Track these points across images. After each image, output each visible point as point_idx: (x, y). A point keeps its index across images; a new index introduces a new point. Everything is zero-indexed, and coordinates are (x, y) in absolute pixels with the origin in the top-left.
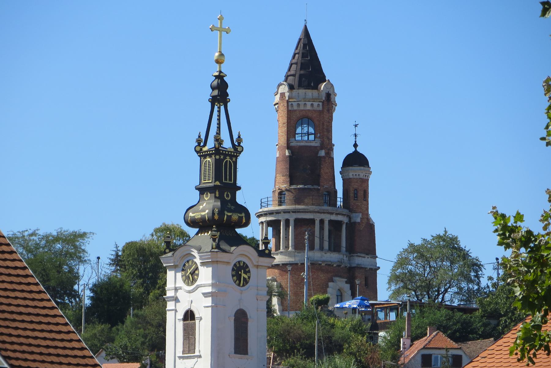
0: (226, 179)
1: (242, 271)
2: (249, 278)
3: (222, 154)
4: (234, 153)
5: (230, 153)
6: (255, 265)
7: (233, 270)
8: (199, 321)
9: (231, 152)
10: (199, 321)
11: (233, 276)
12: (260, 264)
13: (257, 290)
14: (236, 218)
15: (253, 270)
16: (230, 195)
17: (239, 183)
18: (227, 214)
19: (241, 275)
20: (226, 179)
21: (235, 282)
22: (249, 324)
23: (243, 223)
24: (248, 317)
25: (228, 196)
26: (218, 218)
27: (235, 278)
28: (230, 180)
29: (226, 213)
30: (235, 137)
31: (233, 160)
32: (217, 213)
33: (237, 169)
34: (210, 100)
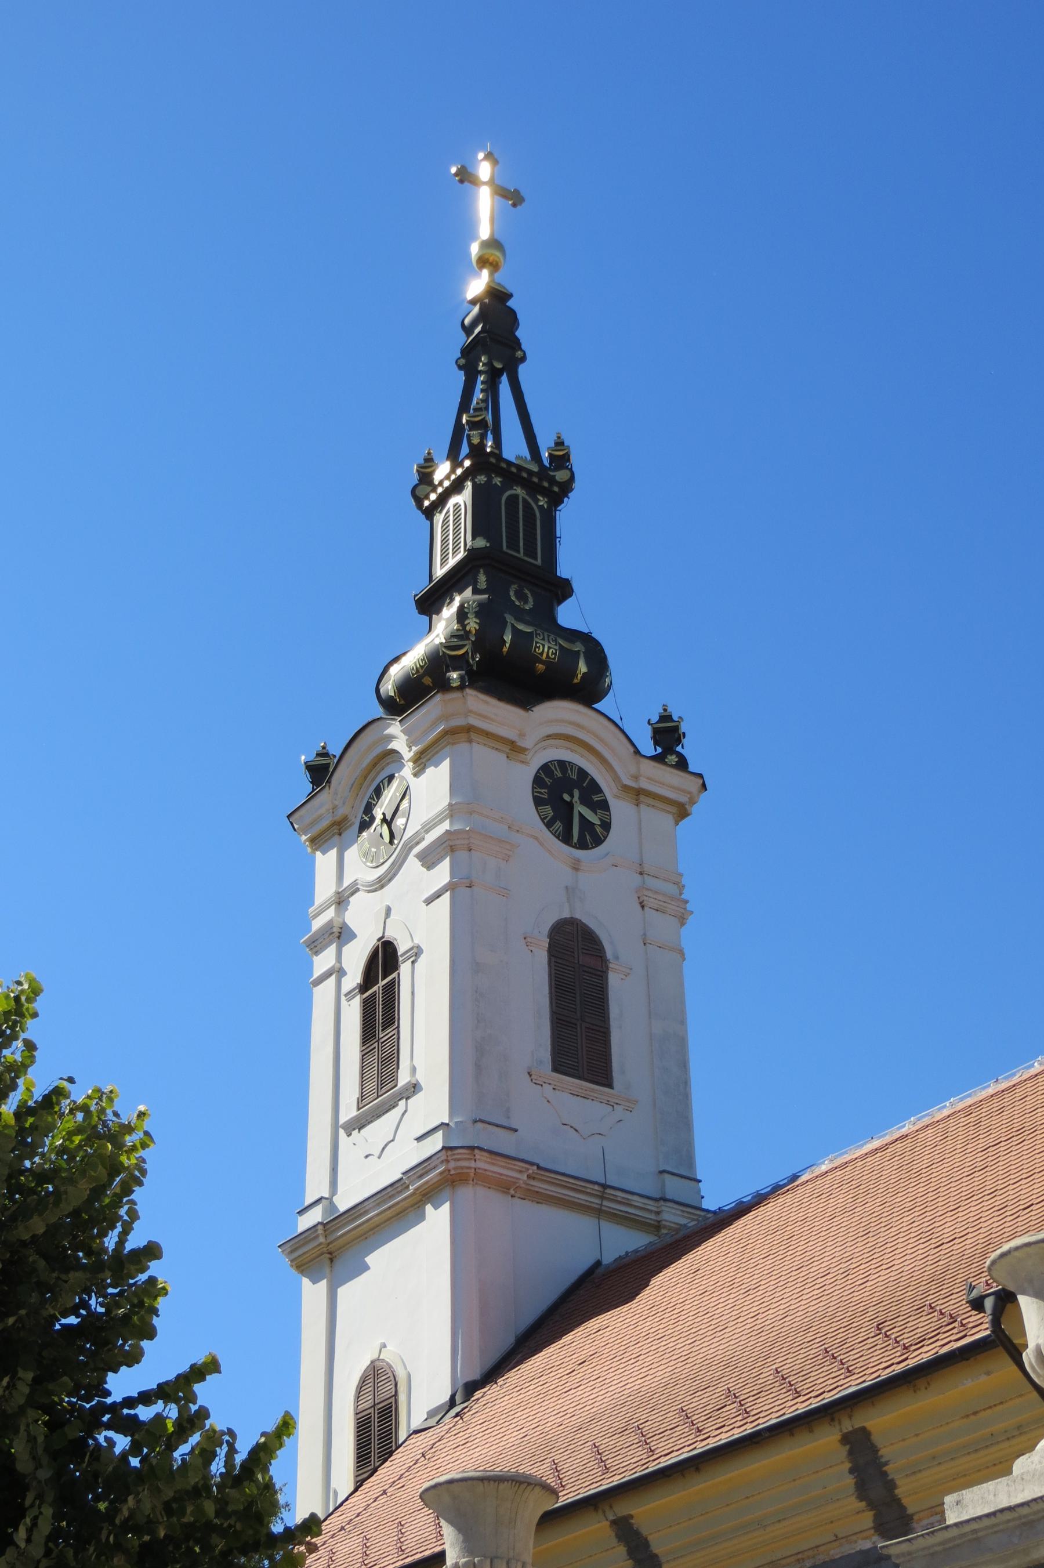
0: (513, 544)
1: (576, 793)
2: (607, 826)
4: (540, 479)
5: (525, 475)
6: (626, 788)
7: (538, 781)
8: (413, 962)
9: (530, 473)
10: (413, 962)
11: (538, 802)
12: (645, 784)
13: (641, 873)
14: (549, 648)
15: (620, 809)
16: (529, 595)
17: (563, 570)
19: (570, 806)
20: (513, 544)
22: (614, 980)
23: (579, 676)
24: (609, 954)
25: (522, 597)
26: (477, 628)
27: (549, 810)
28: (531, 552)
29: (509, 619)
32: (475, 612)
33: (558, 540)
34: (462, 362)
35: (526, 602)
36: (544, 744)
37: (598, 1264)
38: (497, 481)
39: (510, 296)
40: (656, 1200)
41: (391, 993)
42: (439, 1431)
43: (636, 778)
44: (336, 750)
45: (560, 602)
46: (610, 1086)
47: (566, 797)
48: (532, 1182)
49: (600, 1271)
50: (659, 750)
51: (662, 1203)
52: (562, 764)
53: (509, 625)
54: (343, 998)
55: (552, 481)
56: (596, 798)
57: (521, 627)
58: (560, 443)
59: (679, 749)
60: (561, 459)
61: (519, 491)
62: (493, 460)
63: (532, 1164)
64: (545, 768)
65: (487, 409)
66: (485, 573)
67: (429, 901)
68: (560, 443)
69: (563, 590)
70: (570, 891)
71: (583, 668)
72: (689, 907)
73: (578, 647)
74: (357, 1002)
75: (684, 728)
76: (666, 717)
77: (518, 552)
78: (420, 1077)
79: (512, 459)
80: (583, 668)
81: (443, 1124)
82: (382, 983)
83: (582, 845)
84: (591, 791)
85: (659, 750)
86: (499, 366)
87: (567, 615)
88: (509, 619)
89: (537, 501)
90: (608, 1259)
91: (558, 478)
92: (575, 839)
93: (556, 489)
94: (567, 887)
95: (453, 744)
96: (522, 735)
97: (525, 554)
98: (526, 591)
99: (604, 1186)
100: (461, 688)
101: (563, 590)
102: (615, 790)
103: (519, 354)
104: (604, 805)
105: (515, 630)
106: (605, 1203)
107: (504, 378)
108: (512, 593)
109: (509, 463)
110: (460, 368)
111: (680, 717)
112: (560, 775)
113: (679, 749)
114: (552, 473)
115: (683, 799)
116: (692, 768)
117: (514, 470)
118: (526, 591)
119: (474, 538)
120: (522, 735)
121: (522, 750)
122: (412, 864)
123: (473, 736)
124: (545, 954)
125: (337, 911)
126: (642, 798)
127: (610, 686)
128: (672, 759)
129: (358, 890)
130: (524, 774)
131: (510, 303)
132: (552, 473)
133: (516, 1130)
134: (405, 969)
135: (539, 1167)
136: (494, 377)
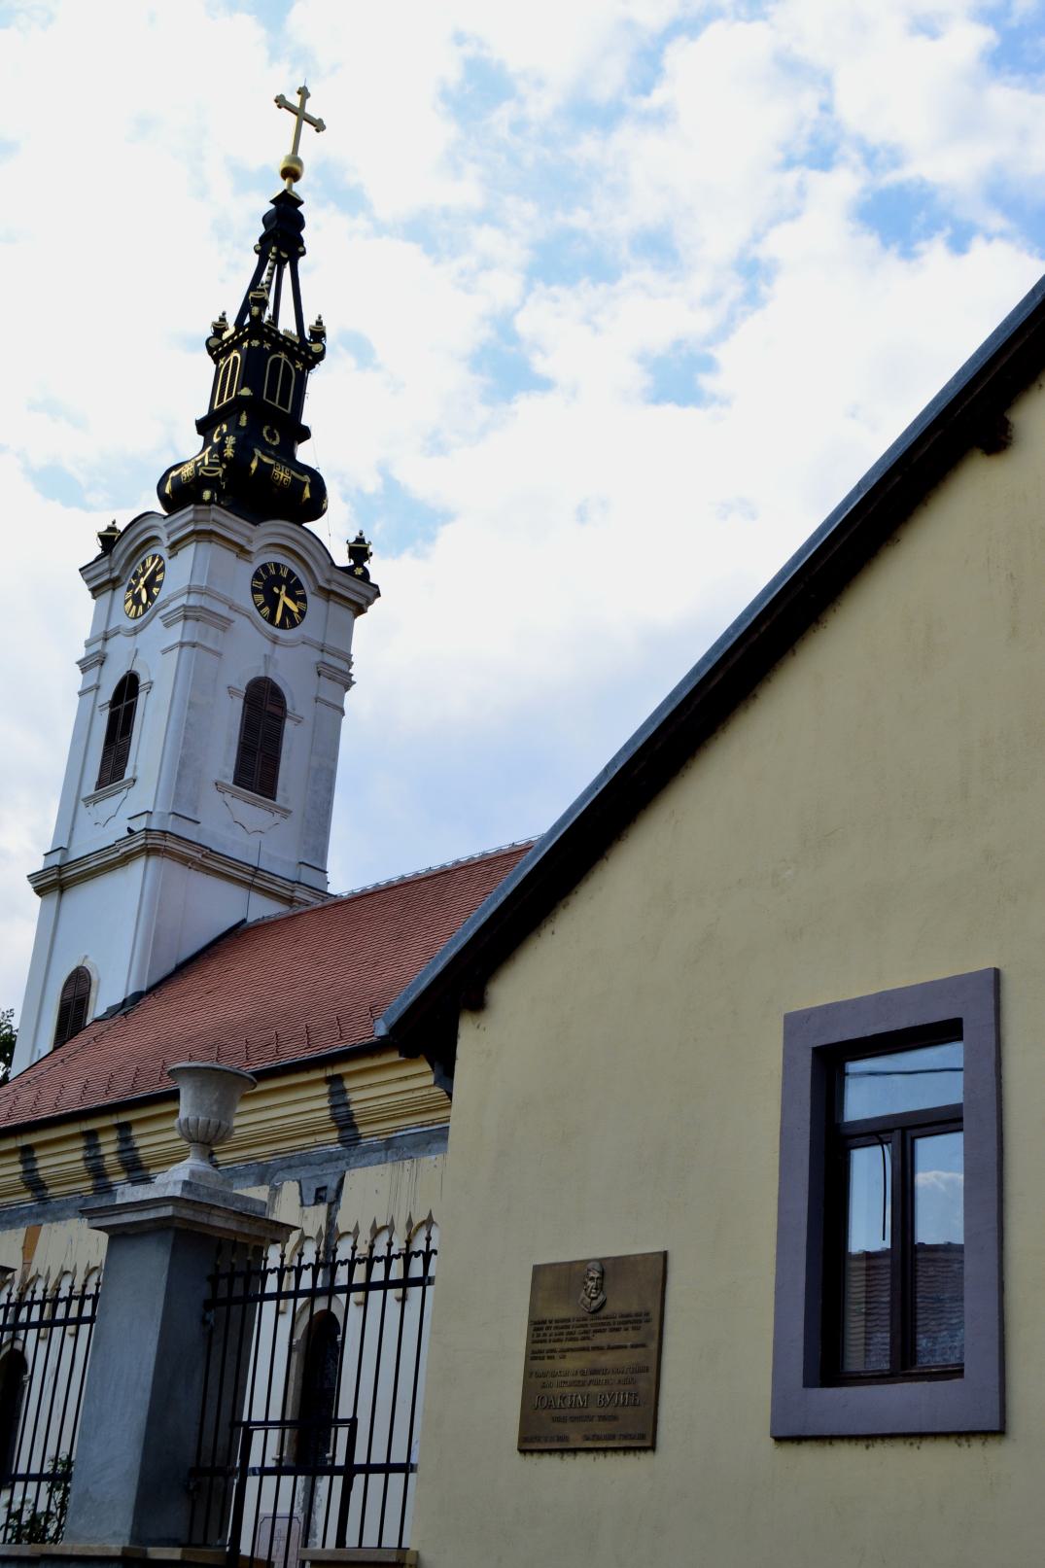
0: (271, 395)
1: (284, 588)
2: (302, 614)
3: (270, 340)
4: (300, 350)
5: (288, 344)
6: (321, 589)
7: (257, 576)
11: (255, 591)
12: (334, 587)
13: (322, 651)
15: (315, 604)
17: (306, 420)
18: (259, 458)
19: (278, 597)
20: (271, 395)
21: (259, 609)
23: (303, 500)
25: (272, 436)
27: (261, 598)
28: (284, 402)
29: (258, 452)
30: (309, 322)
31: (297, 366)
34: (259, 248)
35: (274, 439)
36: (265, 550)
37: (244, 921)
38: (267, 346)
39: (301, 203)
40: (293, 882)
41: (130, 711)
42: (112, 1021)
43: (329, 581)
44: (121, 527)
45: (299, 443)
46: (274, 799)
47: (276, 590)
48: (206, 860)
49: (244, 926)
50: (352, 563)
51: (296, 885)
52: (277, 566)
53: (256, 458)
54: (97, 709)
55: (309, 351)
56: (299, 593)
57: (266, 459)
58: (319, 323)
59: (366, 564)
60: (319, 334)
61: (283, 356)
62: (266, 330)
63: (206, 848)
64: (264, 567)
65: (269, 289)
66: (247, 414)
67: (164, 652)
68: (319, 323)
69: (304, 434)
70: (267, 658)
71: (307, 494)
72: (353, 679)
73: (307, 479)
74: (106, 713)
75: (371, 549)
76: (360, 540)
77: (274, 401)
78: (138, 774)
79: (282, 332)
80: (307, 494)
81: (147, 812)
82: (125, 703)
83: (282, 626)
84: (295, 589)
85: (352, 563)
86: (285, 255)
87: (304, 453)
88: (258, 452)
89: (294, 364)
90: (250, 919)
91: (313, 350)
92: (278, 621)
93: (310, 358)
94: (265, 656)
95: (198, 542)
96: (250, 541)
97: (279, 404)
98: (275, 431)
99: (257, 869)
100: (210, 502)
101: (304, 434)
102: (313, 588)
103: (301, 249)
104: (303, 599)
105: (260, 460)
106: (256, 880)
107: (288, 264)
108: (264, 432)
109: (277, 333)
110: (257, 252)
111: (370, 542)
112: (274, 573)
113: (366, 564)
114: (309, 345)
115: (362, 601)
116: (372, 580)
117: (281, 339)
118: (275, 431)
119: (241, 386)
120: (250, 541)
121: (249, 553)
122: (157, 623)
123: (214, 539)
124: (242, 701)
125: (104, 646)
126: (332, 597)
127: (325, 510)
128: (359, 571)
129: (119, 632)
130: (245, 572)
131: (300, 209)
132: (309, 345)
133: (198, 823)
134: (141, 696)
135: (211, 851)
136: (280, 263)
